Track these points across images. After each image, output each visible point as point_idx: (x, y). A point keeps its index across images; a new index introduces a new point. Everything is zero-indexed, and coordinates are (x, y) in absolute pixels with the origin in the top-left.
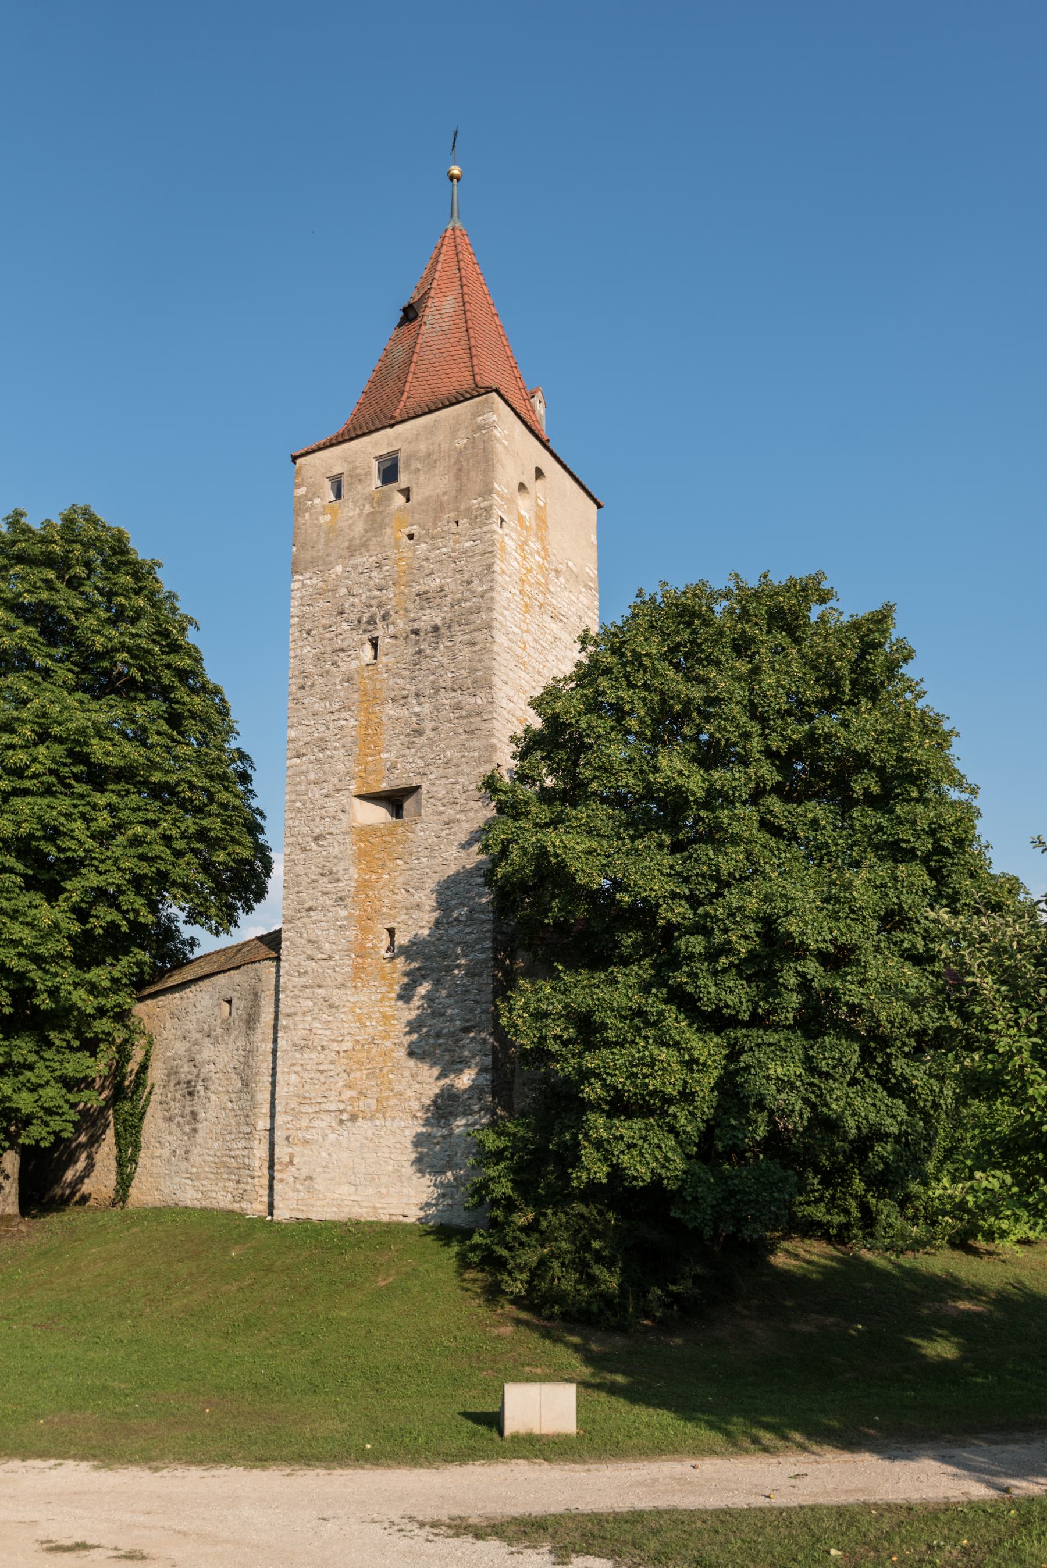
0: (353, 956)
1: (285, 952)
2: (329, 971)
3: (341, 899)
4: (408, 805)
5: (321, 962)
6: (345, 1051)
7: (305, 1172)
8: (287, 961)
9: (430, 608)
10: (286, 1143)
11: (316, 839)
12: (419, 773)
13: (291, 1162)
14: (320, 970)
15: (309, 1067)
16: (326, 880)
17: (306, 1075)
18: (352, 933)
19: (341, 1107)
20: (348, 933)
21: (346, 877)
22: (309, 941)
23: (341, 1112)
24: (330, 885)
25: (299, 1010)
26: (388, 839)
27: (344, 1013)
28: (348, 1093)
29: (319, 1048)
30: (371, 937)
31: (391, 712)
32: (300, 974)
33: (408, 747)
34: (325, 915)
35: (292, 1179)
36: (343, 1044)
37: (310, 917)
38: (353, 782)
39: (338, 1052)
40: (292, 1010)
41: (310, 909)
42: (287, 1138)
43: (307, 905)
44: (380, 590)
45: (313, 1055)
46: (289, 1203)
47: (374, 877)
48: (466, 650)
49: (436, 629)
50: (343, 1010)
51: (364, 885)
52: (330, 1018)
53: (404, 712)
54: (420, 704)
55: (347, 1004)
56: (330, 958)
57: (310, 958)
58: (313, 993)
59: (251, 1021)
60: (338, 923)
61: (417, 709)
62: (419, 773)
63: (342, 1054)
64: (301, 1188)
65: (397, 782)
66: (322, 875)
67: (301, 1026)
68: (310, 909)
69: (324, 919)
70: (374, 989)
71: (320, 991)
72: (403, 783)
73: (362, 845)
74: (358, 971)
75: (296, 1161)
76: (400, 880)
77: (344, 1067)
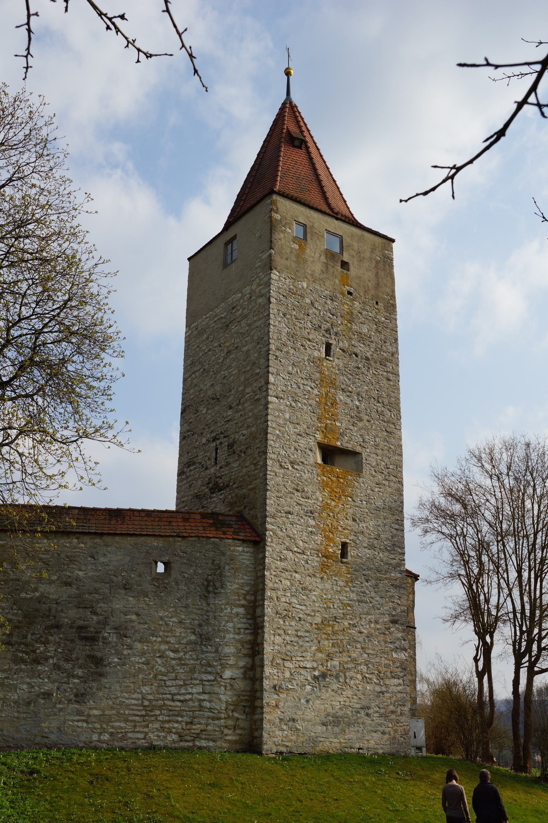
0: (320, 555)
1: (269, 540)
2: (303, 562)
3: (311, 512)
4: (339, 460)
5: (296, 554)
6: (316, 624)
7: (288, 714)
8: (271, 546)
9: (364, 344)
10: (273, 690)
11: (291, 463)
12: (360, 445)
13: (277, 706)
14: (296, 560)
15: (290, 632)
16: (299, 494)
17: (288, 638)
18: (319, 538)
19: (315, 665)
20: (316, 538)
21: (314, 497)
22: (288, 536)
23: (314, 669)
24: (302, 499)
25: (281, 587)
26: (342, 480)
27: (315, 595)
28: (320, 655)
29: (298, 619)
30: (332, 545)
31: (342, 398)
32: (281, 560)
33: (353, 425)
34: (299, 520)
35: (278, 720)
36: (315, 618)
37: (288, 518)
38: (318, 433)
39: (311, 624)
40: (276, 585)
41: (289, 513)
42: (275, 687)
43: (286, 509)
44: (333, 315)
45: (293, 623)
46: (276, 740)
47: (333, 503)
48: (385, 381)
49: (367, 359)
50: (314, 593)
51: (325, 507)
52: (304, 597)
53: (349, 401)
54: (359, 401)
55: (317, 589)
56: (303, 553)
57: (288, 549)
58: (291, 576)
59: (211, 587)
60: (310, 529)
61: (357, 403)
62: (360, 445)
63: (314, 626)
64: (285, 727)
65: (348, 445)
66: (297, 490)
67: (283, 599)
68: (289, 513)
69: (298, 522)
70: (335, 582)
71: (297, 575)
72: (350, 446)
73: (325, 478)
74: (324, 567)
75: (281, 704)
76: (351, 511)
77: (316, 636)
